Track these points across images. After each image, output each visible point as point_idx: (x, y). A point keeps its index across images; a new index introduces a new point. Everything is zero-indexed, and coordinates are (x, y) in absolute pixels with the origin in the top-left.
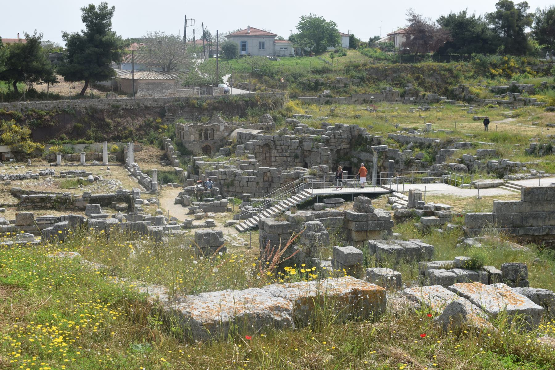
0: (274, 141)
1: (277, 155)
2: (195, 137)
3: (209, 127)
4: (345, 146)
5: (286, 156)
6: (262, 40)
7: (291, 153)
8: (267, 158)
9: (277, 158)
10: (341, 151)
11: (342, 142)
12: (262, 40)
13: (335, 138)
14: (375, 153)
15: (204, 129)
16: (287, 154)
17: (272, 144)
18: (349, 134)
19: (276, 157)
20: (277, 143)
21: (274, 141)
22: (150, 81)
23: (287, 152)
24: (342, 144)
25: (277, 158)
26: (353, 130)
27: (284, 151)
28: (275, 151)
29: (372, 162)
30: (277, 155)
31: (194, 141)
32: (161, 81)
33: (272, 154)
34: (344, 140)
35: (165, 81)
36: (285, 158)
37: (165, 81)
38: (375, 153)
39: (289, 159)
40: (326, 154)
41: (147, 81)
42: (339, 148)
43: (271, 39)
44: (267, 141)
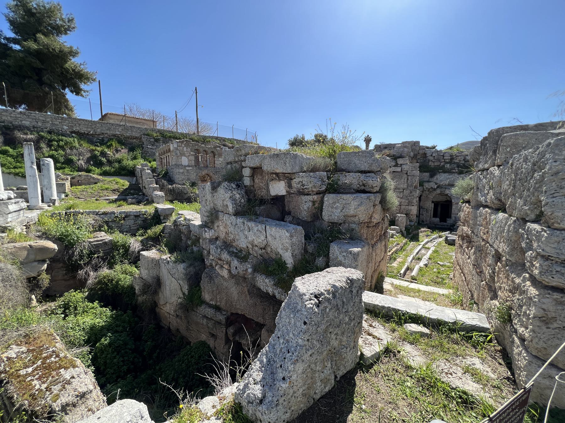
2: (189, 160)
31: (189, 166)
37: (144, 121)
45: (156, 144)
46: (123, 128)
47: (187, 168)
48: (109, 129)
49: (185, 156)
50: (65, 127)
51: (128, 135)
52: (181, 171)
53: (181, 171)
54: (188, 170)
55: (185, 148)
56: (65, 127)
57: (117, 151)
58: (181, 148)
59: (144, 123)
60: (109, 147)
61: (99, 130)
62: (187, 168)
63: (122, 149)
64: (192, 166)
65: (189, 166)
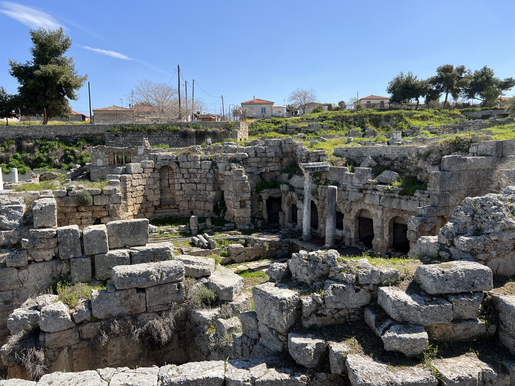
0: (178, 163)
1: (183, 181)
2: (103, 162)
3: (123, 149)
4: (272, 168)
5: (195, 183)
6: (263, 106)
7: (201, 178)
8: (171, 186)
9: (183, 186)
10: (267, 175)
11: (267, 162)
12: (263, 106)
13: (256, 156)
14: (307, 175)
15: (116, 152)
16: (196, 180)
17: (174, 166)
18: (278, 150)
19: (182, 184)
20: (181, 164)
21: (178, 163)
22: (107, 112)
23: (195, 177)
24: (269, 165)
25: (183, 186)
26: (283, 145)
27: (192, 175)
28: (179, 176)
29: (303, 189)
30: (183, 181)
31: (103, 166)
32: (118, 113)
33: (176, 180)
34: (270, 160)
35: (122, 112)
36: (194, 185)
37: (122, 112)
38: (307, 175)
39: (199, 186)
40: (239, 178)
41: (103, 112)
42: (264, 171)
43: (270, 105)
44: (167, 161)
45: (116, 138)
46: (91, 127)
47: (101, 168)
48: (81, 130)
49: (99, 158)
50: (52, 133)
51: (95, 133)
52: (96, 170)
53: (96, 170)
54: (102, 170)
55: (100, 153)
56: (52, 133)
57: (84, 149)
58: (96, 153)
59: (123, 114)
60: (78, 146)
61: (74, 132)
62: (101, 168)
63: (88, 146)
64: (106, 166)
65: (103, 166)
